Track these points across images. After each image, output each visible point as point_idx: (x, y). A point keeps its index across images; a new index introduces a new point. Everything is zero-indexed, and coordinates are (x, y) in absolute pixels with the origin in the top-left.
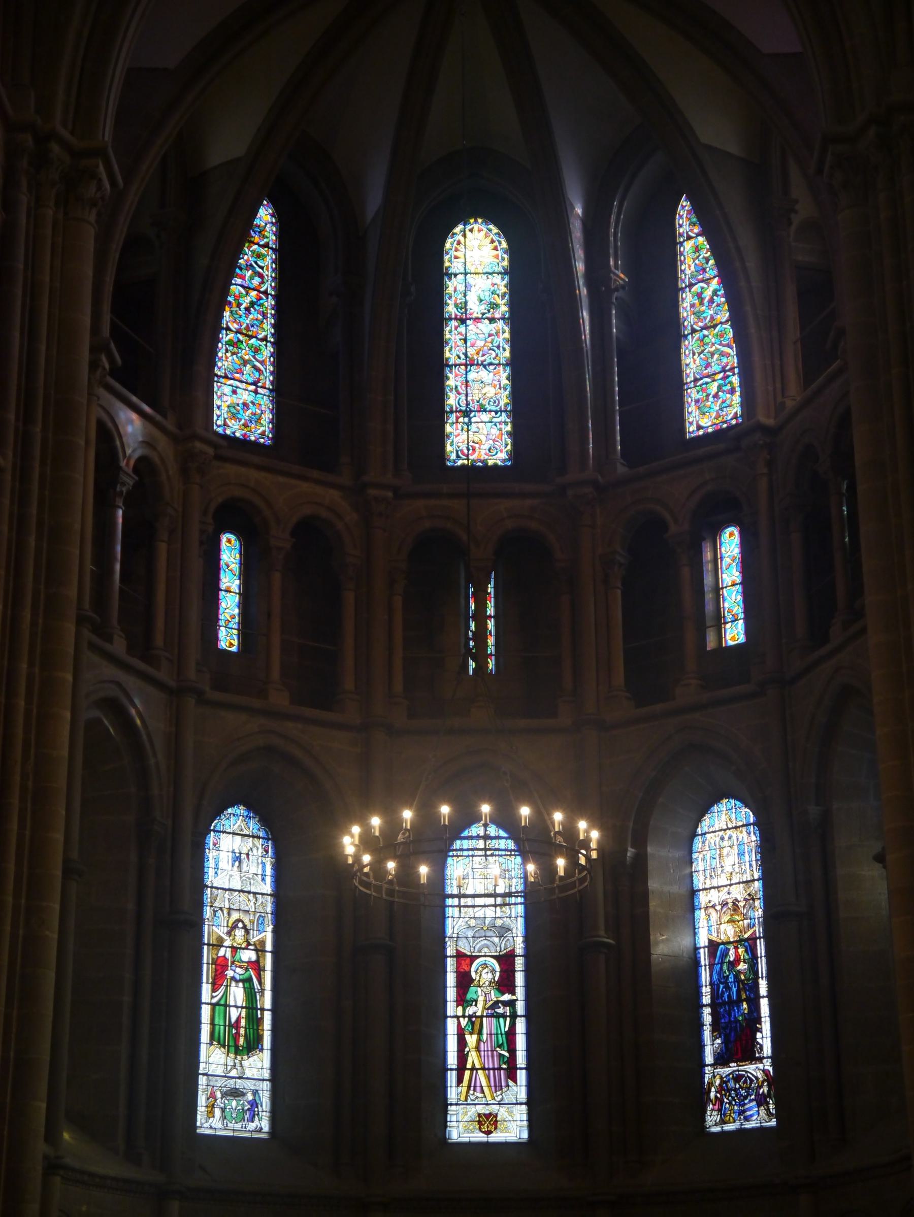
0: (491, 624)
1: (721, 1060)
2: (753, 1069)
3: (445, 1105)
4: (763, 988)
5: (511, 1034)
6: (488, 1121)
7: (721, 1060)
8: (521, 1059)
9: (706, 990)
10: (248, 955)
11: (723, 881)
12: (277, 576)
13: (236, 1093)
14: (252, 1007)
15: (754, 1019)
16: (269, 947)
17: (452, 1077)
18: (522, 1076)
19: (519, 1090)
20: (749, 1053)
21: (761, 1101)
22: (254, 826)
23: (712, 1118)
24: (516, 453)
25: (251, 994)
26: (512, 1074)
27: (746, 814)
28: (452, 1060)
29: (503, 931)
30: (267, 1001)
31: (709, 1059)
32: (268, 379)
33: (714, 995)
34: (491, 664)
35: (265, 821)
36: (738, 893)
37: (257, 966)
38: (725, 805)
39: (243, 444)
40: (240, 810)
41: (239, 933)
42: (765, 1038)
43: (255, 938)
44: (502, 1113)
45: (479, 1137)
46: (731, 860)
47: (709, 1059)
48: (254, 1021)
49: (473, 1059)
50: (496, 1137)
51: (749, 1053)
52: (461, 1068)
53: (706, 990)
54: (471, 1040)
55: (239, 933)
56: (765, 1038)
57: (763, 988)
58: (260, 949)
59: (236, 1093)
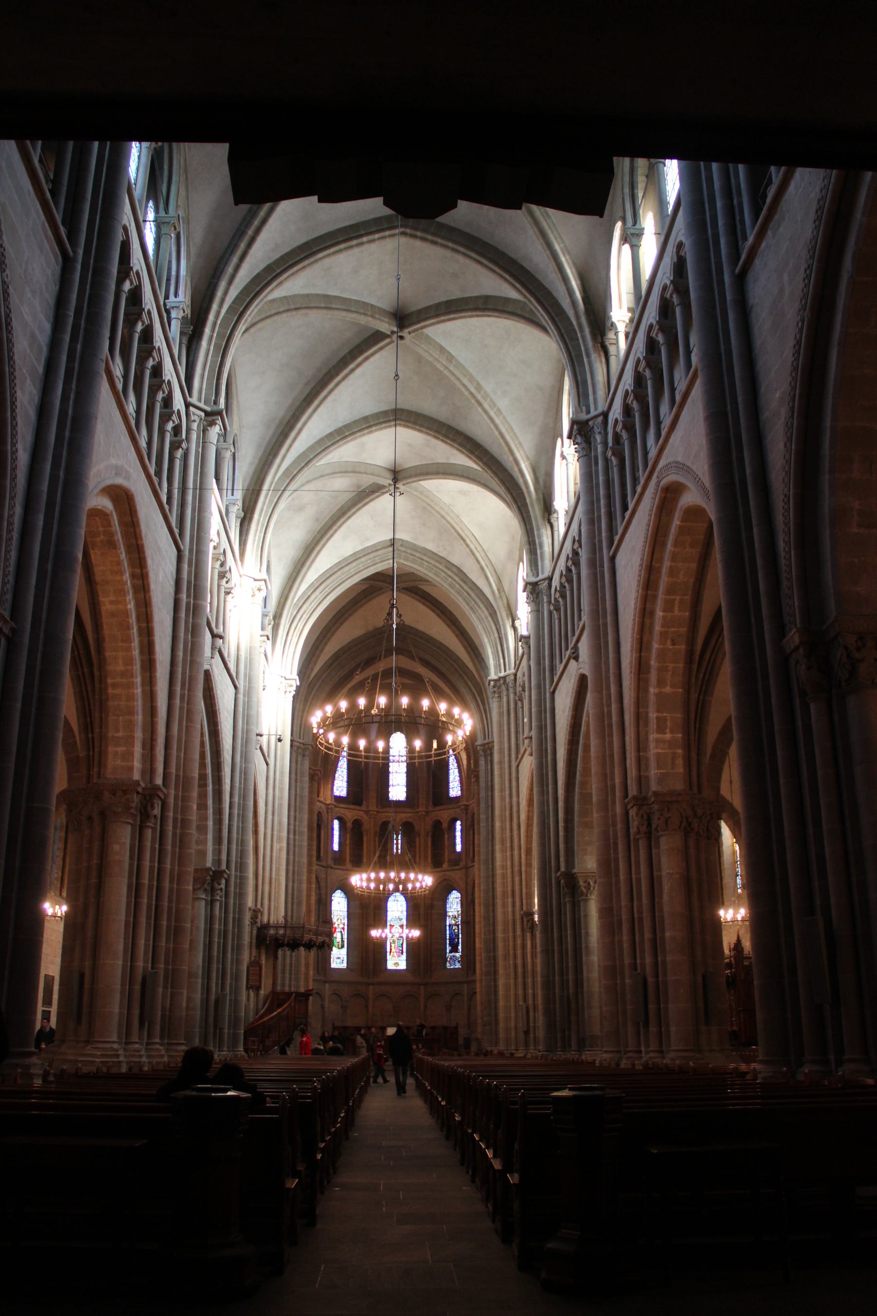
0: (400, 841)
1: (451, 952)
2: (458, 955)
3: (386, 960)
4: (460, 936)
5: (402, 944)
6: (397, 964)
7: (451, 952)
8: (405, 950)
9: (448, 935)
10: (342, 926)
11: (452, 910)
12: (348, 836)
13: (339, 958)
14: (342, 938)
15: (458, 943)
16: (346, 924)
17: (388, 954)
18: (405, 954)
19: (404, 957)
20: (456, 951)
21: (459, 962)
22: (343, 895)
23: (448, 965)
24: (407, 797)
25: (342, 935)
26: (402, 953)
27: (459, 895)
28: (388, 950)
29: (401, 919)
30: (345, 936)
31: (448, 951)
32: (345, 779)
33: (450, 937)
34: (399, 851)
35: (345, 894)
36: (456, 914)
37: (343, 929)
38: (454, 892)
39: (340, 797)
40: (339, 891)
41: (339, 921)
42: (460, 947)
43: (343, 922)
44: (400, 962)
45: (394, 968)
46: (455, 906)
47: (448, 951)
48: (343, 941)
49: (393, 950)
50: (398, 968)
51: (456, 951)
52: (390, 952)
53: (448, 935)
54: (393, 945)
55: (339, 921)
56: (460, 947)
57: (460, 936)
58: (344, 925)
59: (339, 958)
